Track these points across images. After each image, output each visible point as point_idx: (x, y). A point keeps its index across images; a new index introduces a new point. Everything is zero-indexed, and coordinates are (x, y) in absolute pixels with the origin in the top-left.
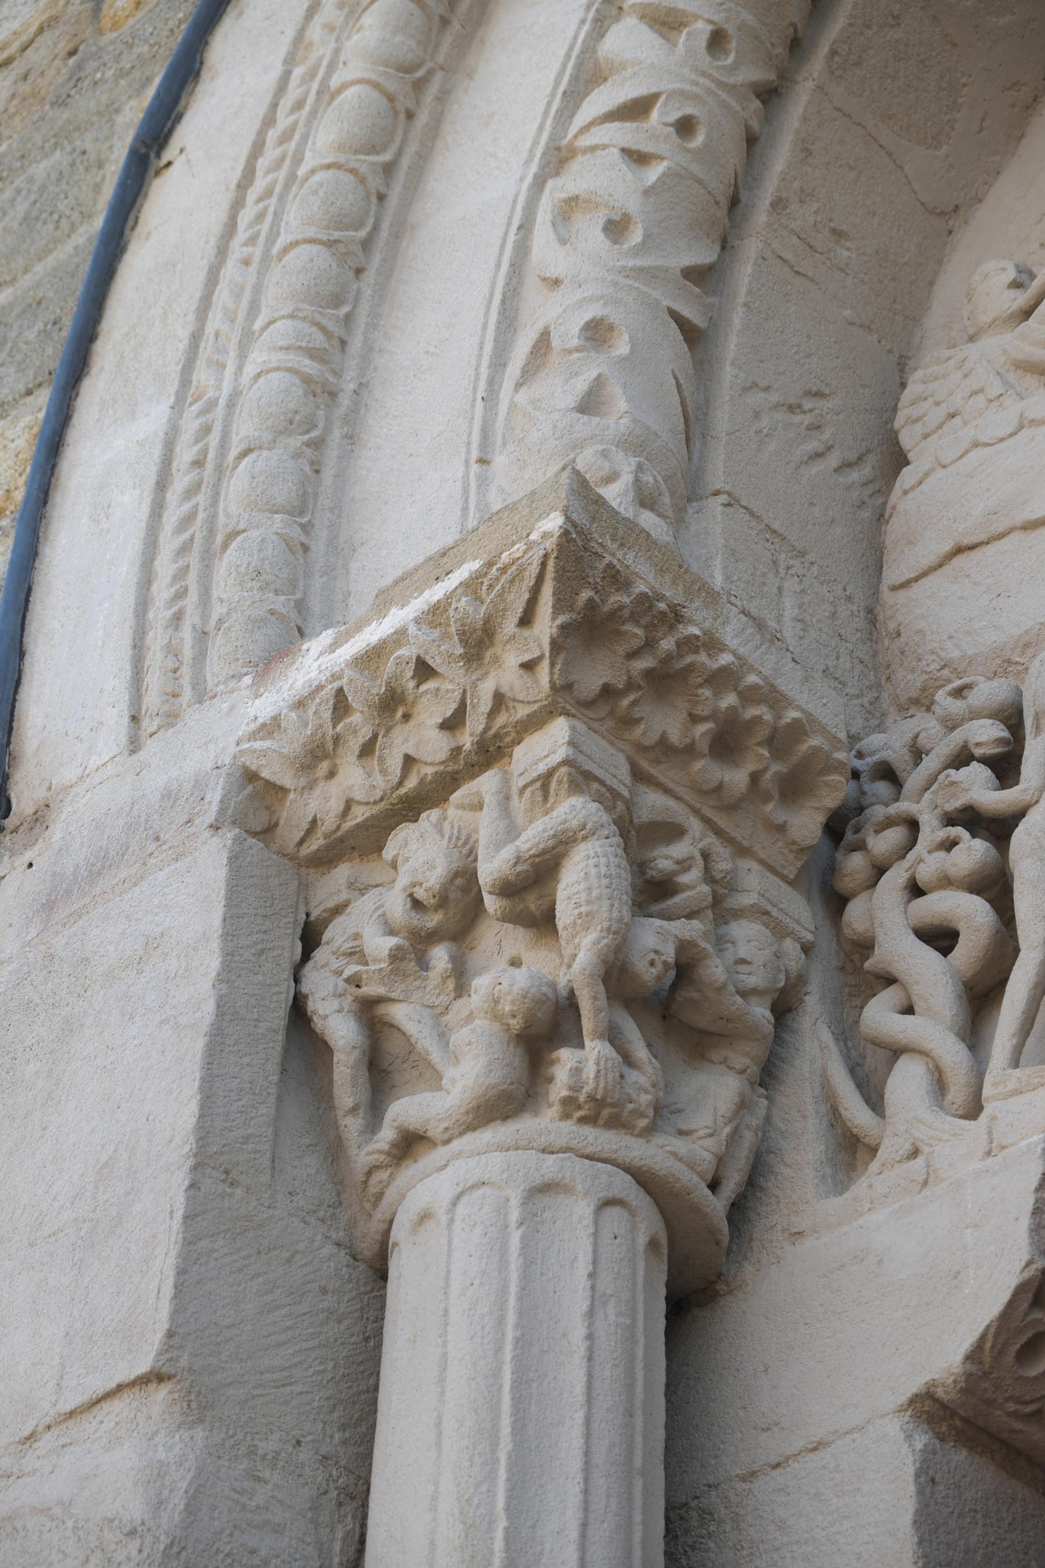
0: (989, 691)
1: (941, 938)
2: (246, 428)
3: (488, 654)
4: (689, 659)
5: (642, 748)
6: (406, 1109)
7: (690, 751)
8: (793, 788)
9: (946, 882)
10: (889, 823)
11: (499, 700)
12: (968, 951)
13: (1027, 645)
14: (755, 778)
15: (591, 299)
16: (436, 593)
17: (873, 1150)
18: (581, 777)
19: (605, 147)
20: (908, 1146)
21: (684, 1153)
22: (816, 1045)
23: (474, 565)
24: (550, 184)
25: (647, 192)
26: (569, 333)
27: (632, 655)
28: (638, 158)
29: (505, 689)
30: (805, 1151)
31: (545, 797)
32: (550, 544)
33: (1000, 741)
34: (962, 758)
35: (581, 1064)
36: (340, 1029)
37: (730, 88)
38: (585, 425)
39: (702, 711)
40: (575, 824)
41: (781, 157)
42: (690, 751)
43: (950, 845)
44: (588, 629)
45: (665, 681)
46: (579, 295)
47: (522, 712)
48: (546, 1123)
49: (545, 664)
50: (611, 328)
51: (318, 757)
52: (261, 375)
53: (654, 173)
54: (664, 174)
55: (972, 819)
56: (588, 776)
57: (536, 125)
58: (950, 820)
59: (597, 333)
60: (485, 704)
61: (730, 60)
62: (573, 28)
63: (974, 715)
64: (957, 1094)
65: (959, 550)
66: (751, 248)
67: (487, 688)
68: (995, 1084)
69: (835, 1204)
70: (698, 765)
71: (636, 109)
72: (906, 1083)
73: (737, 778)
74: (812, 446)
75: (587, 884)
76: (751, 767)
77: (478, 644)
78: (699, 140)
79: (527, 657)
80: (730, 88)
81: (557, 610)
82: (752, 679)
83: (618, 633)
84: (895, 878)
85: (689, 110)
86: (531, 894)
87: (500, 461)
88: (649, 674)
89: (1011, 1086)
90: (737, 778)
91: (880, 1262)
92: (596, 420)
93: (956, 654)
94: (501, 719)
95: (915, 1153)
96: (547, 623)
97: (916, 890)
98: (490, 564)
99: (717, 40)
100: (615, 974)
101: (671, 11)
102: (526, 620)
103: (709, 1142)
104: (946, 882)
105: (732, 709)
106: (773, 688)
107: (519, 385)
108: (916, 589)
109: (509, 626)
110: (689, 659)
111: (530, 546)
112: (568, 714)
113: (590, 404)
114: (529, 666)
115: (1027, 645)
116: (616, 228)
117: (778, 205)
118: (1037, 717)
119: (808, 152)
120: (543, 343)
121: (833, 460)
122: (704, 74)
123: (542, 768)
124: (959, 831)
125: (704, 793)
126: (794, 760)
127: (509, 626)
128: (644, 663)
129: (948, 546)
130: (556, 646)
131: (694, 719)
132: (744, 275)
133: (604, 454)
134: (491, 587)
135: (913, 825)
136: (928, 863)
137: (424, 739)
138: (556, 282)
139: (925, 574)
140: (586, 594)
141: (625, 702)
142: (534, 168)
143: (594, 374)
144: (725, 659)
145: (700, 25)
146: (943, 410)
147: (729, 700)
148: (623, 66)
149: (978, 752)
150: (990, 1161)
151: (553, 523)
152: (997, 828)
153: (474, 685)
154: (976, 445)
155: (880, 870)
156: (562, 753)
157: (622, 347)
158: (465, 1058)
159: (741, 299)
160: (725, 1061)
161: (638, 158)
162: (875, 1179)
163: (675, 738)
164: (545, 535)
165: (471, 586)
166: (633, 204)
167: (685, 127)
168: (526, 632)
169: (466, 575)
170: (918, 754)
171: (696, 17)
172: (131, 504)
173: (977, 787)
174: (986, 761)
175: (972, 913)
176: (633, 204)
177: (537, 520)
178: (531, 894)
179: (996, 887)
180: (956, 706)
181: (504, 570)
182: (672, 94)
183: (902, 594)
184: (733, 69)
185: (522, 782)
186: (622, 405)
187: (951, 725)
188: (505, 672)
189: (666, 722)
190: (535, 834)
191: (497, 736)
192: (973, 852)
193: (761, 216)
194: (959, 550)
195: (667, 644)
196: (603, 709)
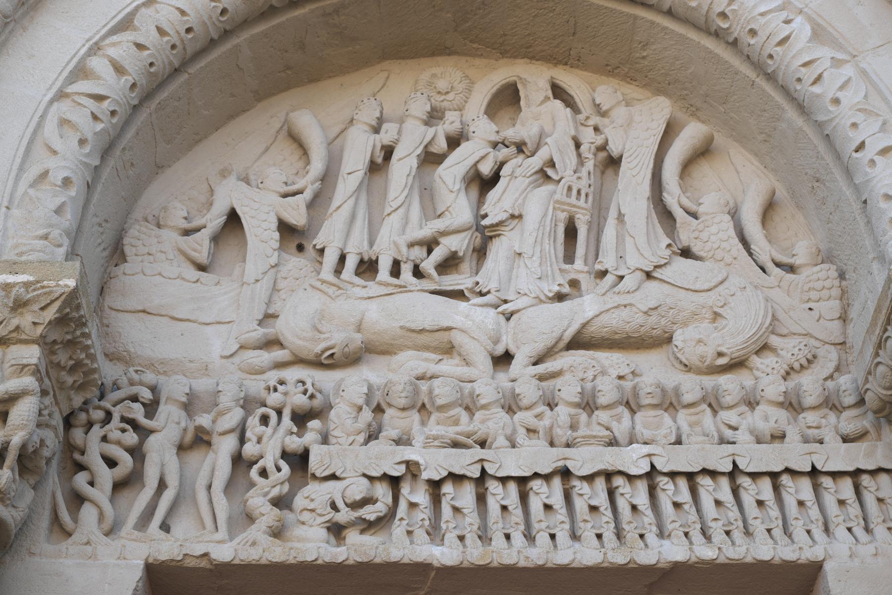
0: (150, 377)
1: (111, 463)
3: (20, 310)
4: (81, 339)
5: (51, 362)
7: (64, 368)
8: (81, 387)
9: (118, 443)
10: (99, 408)
11: (17, 328)
12: (120, 472)
13: (162, 363)
14: (75, 382)
15: (68, 168)
16: (11, 279)
17: (69, 535)
18: (36, 372)
19: (85, 107)
20: (85, 540)
22: (53, 482)
23: (31, 279)
24: (56, 104)
25: (95, 133)
26: (57, 177)
27: (67, 333)
28: (95, 117)
29: (22, 326)
31: (20, 372)
32: (67, 290)
33: (151, 400)
34: (135, 399)
37: (128, 102)
38: (55, 219)
39: (75, 357)
40: (31, 388)
41: (130, 134)
42: (64, 368)
43: (123, 431)
44: (62, 321)
45: (71, 344)
46: (63, 163)
47: (24, 337)
49: (42, 327)
50: (71, 182)
53: (99, 127)
54: (102, 129)
55: (134, 425)
56: (39, 371)
57: (55, 76)
58: (123, 419)
59: (67, 182)
60: (11, 327)
61: (133, 95)
62: (79, 46)
63: (141, 383)
64: (106, 526)
65: (144, 311)
66: (111, 162)
67: (15, 322)
68: (127, 534)
69: (49, 548)
70: (63, 373)
71: (99, 98)
72: (88, 513)
73: (70, 380)
74: (99, 241)
76: (76, 378)
78: (114, 120)
79: (36, 321)
80: (128, 102)
81: (57, 311)
82: (92, 351)
83: (68, 325)
84: (97, 431)
85: (117, 109)
87: (15, 212)
88: (69, 341)
89: (134, 537)
90: (70, 380)
91: (67, 580)
92: (59, 218)
93: (132, 350)
94: (14, 335)
95: (88, 543)
96: (51, 314)
97: (104, 439)
98: (38, 282)
99: (134, 86)
101: (121, 66)
102: (42, 309)
103: (21, 513)
104: (118, 443)
105: (83, 359)
106: (95, 356)
107: (31, 186)
108: (120, 315)
109: (36, 307)
110: (81, 339)
111: (58, 285)
112: (39, 345)
113: (58, 211)
114: (35, 324)
115: (162, 363)
116: (82, 142)
117: (124, 149)
118: (167, 399)
119: (138, 133)
120: (45, 175)
121: (102, 248)
122: (125, 97)
123: (25, 361)
124: (128, 427)
125: (58, 382)
126: (87, 379)
127: (36, 307)
128: (69, 337)
129: (140, 308)
130: (50, 322)
131: (71, 358)
132: (106, 173)
133: (61, 235)
134: (34, 290)
135: (109, 415)
136: (115, 435)
138: (55, 152)
139: (127, 312)
140: (68, 310)
141: (57, 347)
142: (50, 95)
143: (63, 200)
144: (89, 342)
145: (130, 78)
146: (146, 250)
147: (83, 356)
148: (99, 78)
149: (141, 400)
150: (119, 562)
151: (71, 283)
152: (144, 432)
153: (10, 319)
154: (160, 274)
155: (90, 425)
156: (34, 361)
157: (73, 192)
159: (103, 181)
160: (28, 480)
161: (95, 117)
162: (68, 546)
163: (62, 363)
164: (66, 286)
165: (27, 285)
166: (90, 136)
167: (113, 113)
168: (41, 313)
169: (25, 280)
170: (116, 386)
171: (130, 75)
173: (137, 412)
174: (144, 404)
175: (126, 462)
176: (90, 136)
177: (64, 277)
179: (137, 453)
180: (136, 377)
181: (43, 287)
182: (114, 100)
183: (114, 313)
184: (133, 98)
185: (13, 362)
186: (69, 216)
187: (132, 383)
188: (26, 320)
189: (62, 357)
191: (9, 339)
192: (131, 438)
193: (117, 152)
194: (144, 311)
195: (78, 333)
196: (48, 346)
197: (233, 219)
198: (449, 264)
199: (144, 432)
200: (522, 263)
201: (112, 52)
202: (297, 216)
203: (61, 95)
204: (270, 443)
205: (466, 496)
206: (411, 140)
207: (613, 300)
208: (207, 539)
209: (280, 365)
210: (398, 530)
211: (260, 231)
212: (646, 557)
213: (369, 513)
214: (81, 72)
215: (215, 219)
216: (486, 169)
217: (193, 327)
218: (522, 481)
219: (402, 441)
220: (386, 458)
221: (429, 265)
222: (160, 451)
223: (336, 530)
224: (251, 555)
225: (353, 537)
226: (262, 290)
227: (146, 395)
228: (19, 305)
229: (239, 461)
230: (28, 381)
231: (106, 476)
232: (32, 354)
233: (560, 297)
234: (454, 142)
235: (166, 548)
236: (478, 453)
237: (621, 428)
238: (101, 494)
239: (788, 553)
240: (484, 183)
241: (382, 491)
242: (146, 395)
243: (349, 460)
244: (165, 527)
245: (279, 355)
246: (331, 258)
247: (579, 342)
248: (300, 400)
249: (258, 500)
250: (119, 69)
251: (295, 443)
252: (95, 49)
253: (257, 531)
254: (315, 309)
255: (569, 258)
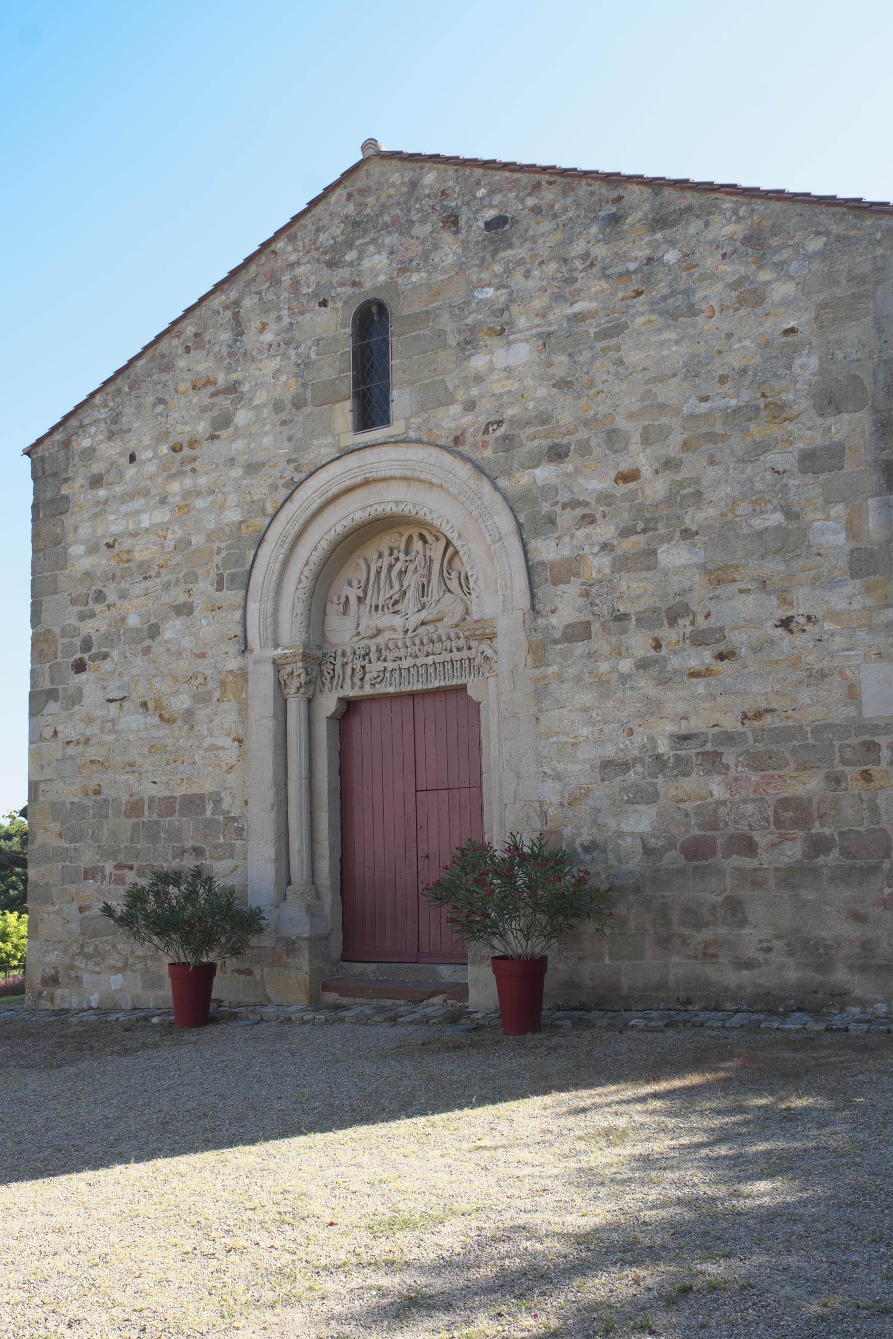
2: (269, 615)
6: (288, 691)
21: (309, 695)
30: (318, 691)
35: (302, 690)
36: (283, 683)
48: (299, 694)
51: (279, 659)
52: (269, 606)
72: (326, 687)
75: (303, 676)
77: (294, 656)
86: (299, 676)
100: (305, 683)
137: (290, 660)
152: (334, 665)
158: (293, 690)
172: (256, 615)
173: (332, 659)
175: (332, 672)
178: (299, 676)
179: (334, 670)
190: (299, 672)
192: (332, 667)
197: (347, 598)
198: (396, 602)
199: (334, 665)
200: (410, 604)
201: (306, 573)
202: (361, 595)
203: (297, 589)
204: (358, 664)
205: (396, 675)
206: (386, 561)
207: (430, 611)
208: (349, 692)
209: (361, 640)
210: (384, 684)
211: (353, 601)
212: (431, 686)
213: (378, 680)
214: (300, 581)
215: (343, 600)
216: (403, 569)
217: (342, 632)
218: (408, 669)
219: (385, 660)
220: (380, 665)
221: (390, 606)
222: (338, 668)
223: (373, 685)
224: (356, 694)
225: (377, 686)
226: (356, 618)
227: (333, 655)
228: (294, 656)
229: (353, 670)
230: (302, 670)
231: (328, 677)
232: (300, 664)
233: (419, 611)
234: (397, 559)
235: (342, 693)
236: (398, 662)
237: (430, 651)
238: (327, 682)
239: (460, 682)
240: (402, 573)
241: (381, 674)
242: (333, 655)
243: (374, 668)
244: (342, 687)
245: (360, 637)
246: (368, 607)
247: (423, 624)
248: (363, 652)
249: (357, 680)
250: (307, 578)
251: (362, 664)
252: (302, 573)
253: (356, 688)
254: (370, 621)
255: (423, 596)
